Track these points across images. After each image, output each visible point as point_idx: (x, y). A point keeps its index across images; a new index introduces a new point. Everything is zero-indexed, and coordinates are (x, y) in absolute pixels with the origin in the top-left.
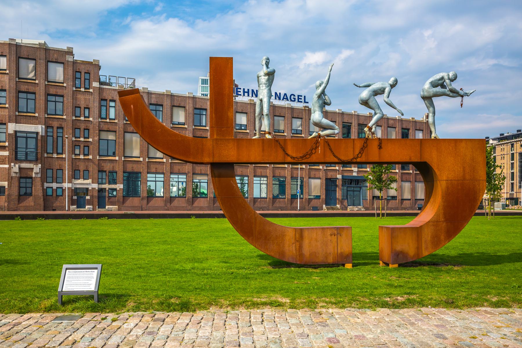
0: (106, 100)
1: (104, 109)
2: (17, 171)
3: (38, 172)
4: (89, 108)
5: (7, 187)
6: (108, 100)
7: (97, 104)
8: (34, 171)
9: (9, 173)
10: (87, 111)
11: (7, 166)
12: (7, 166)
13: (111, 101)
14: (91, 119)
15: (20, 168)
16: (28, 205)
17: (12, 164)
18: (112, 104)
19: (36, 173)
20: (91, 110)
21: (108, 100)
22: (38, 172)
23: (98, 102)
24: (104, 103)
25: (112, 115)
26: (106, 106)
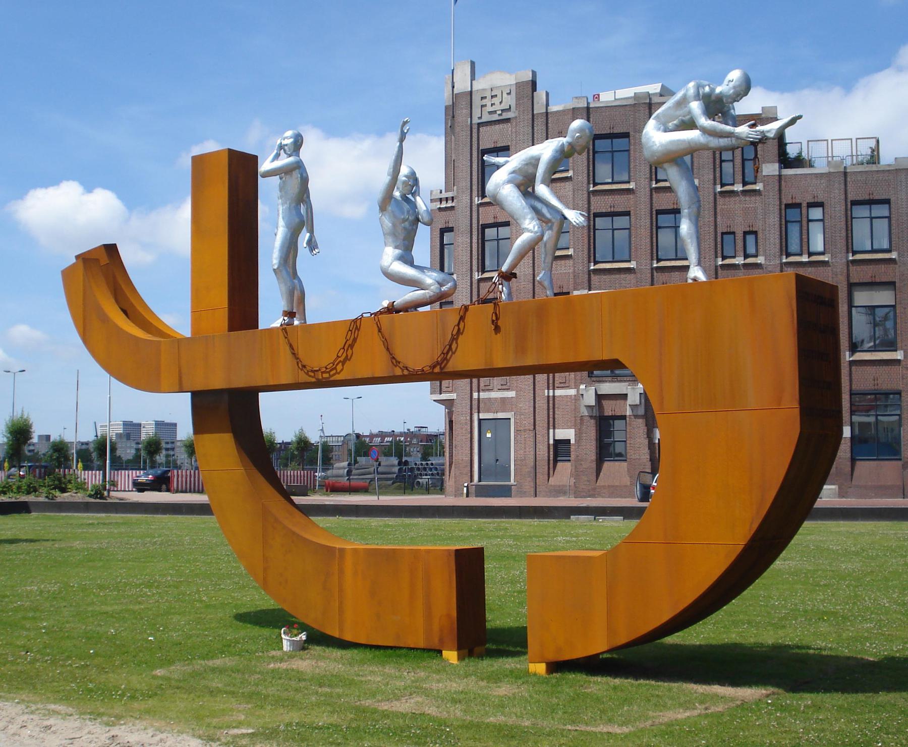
0: (798, 206)
1: (794, 230)
2: (592, 402)
3: (638, 402)
4: (755, 233)
5: (573, 441)
6: (804, 205)
7: (773, 220)
8: (630, 401)
9: (576, 409)
10: (750, 239)
11: (572, 392)
12: (572, 392)
13: (811, 205)
14: (760, 260)
15: (600, 398)
16: (617, 484)
17: (582, 387)
18: (816, 213)
19: (633, 407)
20: (760, 235)
21: (804, 205)
22: (638, 402)
23: (777, 215)
24: (793, 214)
25: (818, 242)
26: (800, 222)
